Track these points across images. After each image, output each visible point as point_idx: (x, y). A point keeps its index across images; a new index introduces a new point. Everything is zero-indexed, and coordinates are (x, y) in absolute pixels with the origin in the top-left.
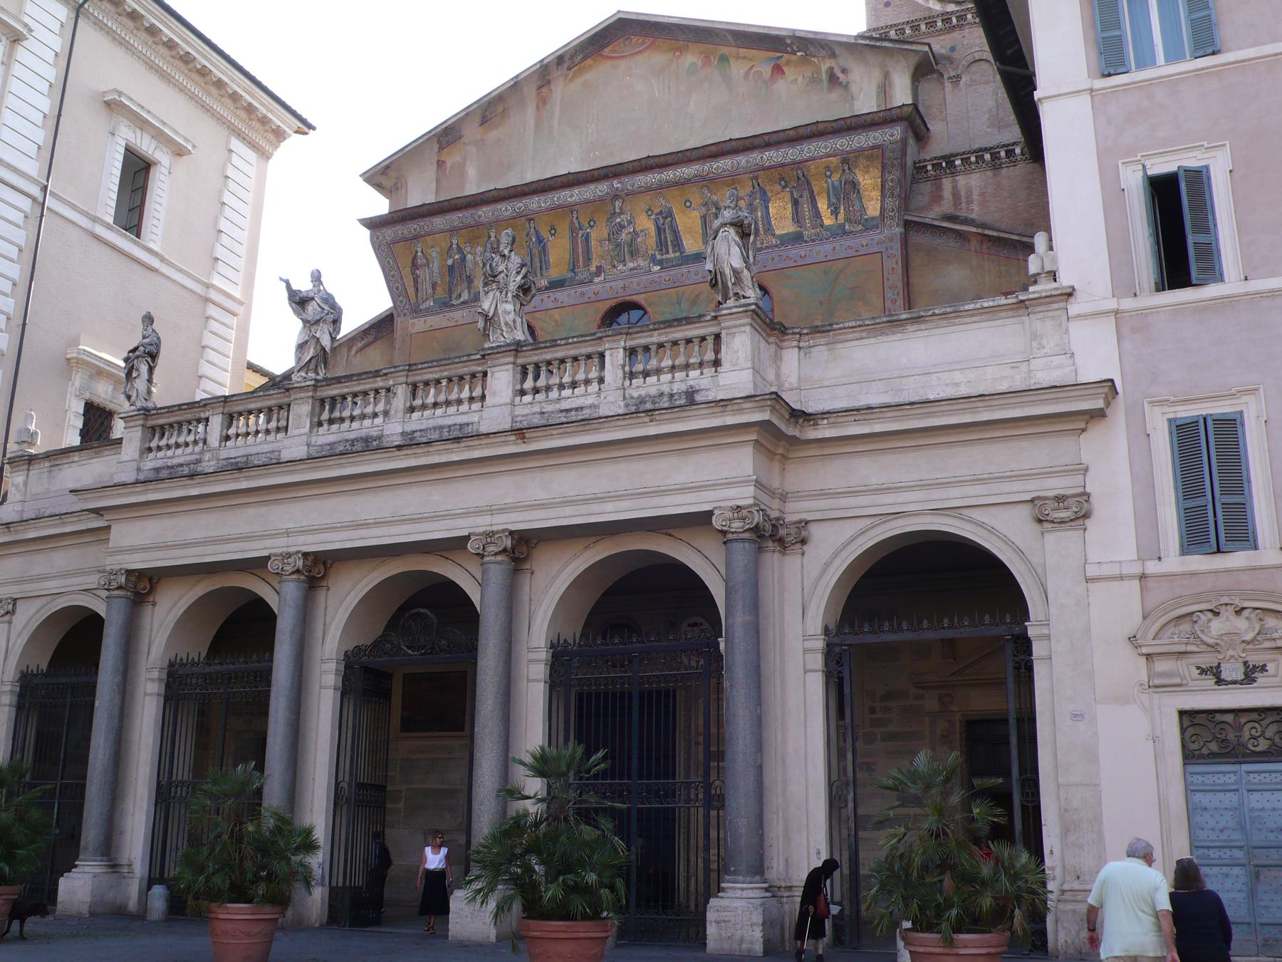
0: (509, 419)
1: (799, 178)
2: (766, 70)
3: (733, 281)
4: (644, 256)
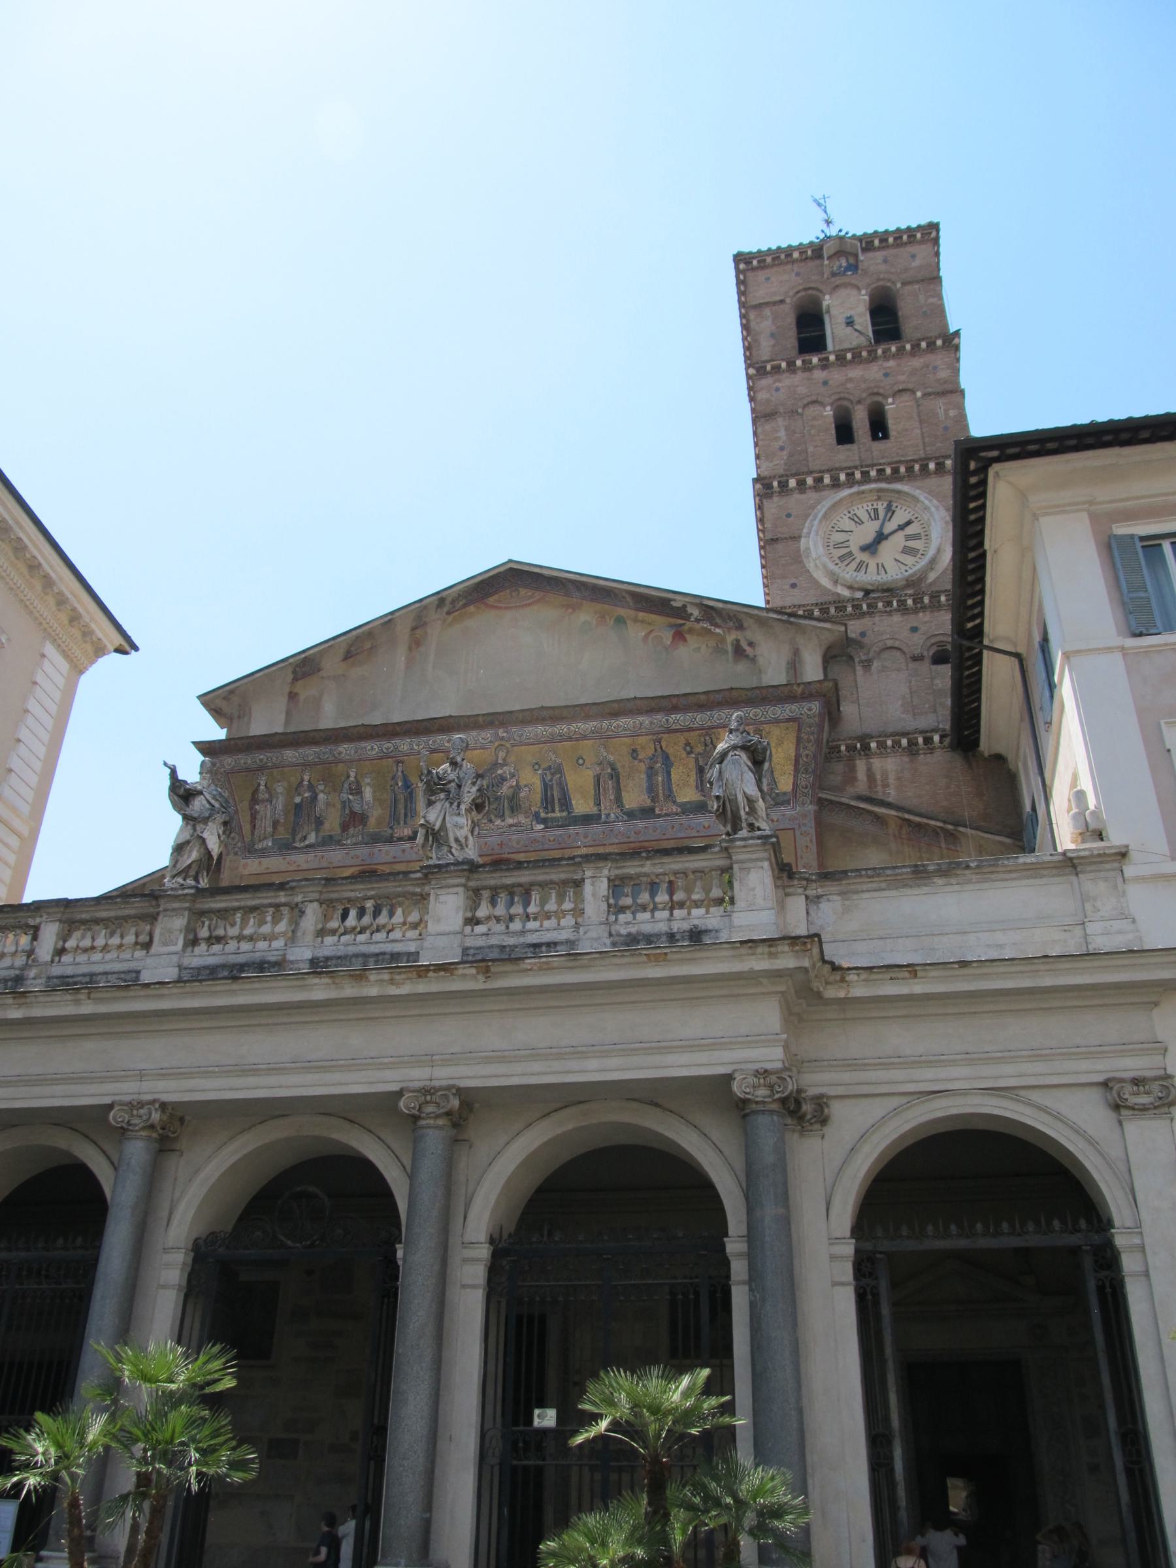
0: (459, 951)
1: (706, 745)
2: (667, 637)
3: (747, 809)
4: (526, 812)
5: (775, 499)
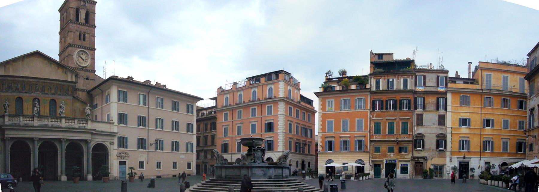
2: (57, 68)
5: (71, 47)
